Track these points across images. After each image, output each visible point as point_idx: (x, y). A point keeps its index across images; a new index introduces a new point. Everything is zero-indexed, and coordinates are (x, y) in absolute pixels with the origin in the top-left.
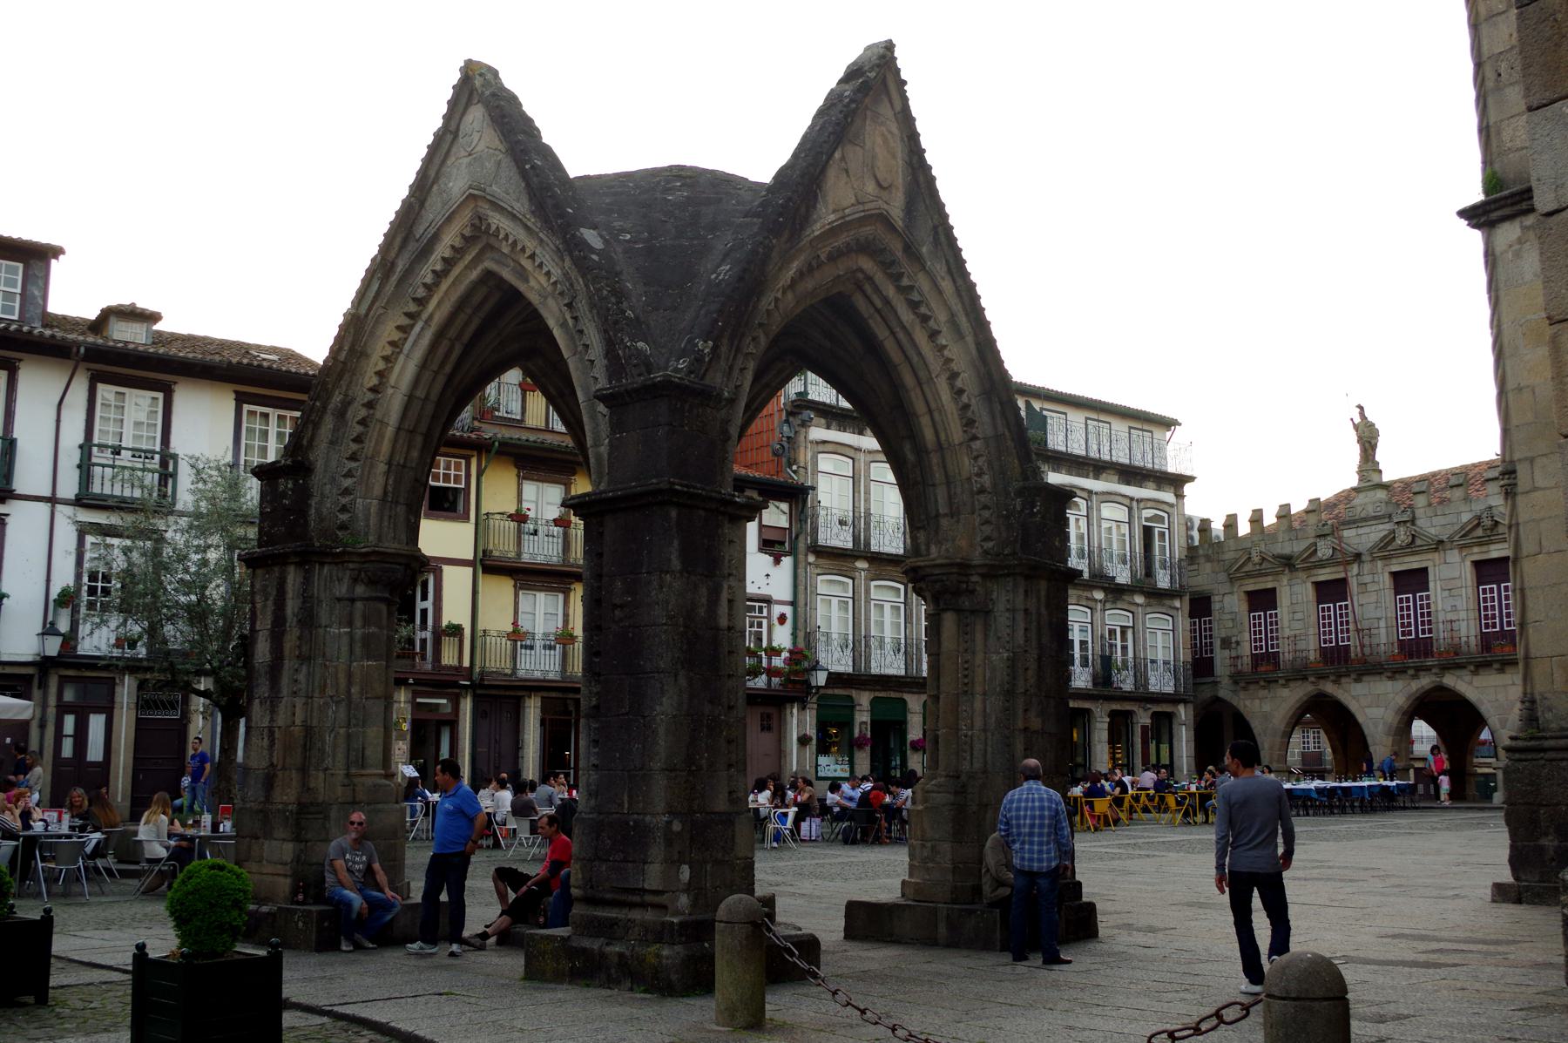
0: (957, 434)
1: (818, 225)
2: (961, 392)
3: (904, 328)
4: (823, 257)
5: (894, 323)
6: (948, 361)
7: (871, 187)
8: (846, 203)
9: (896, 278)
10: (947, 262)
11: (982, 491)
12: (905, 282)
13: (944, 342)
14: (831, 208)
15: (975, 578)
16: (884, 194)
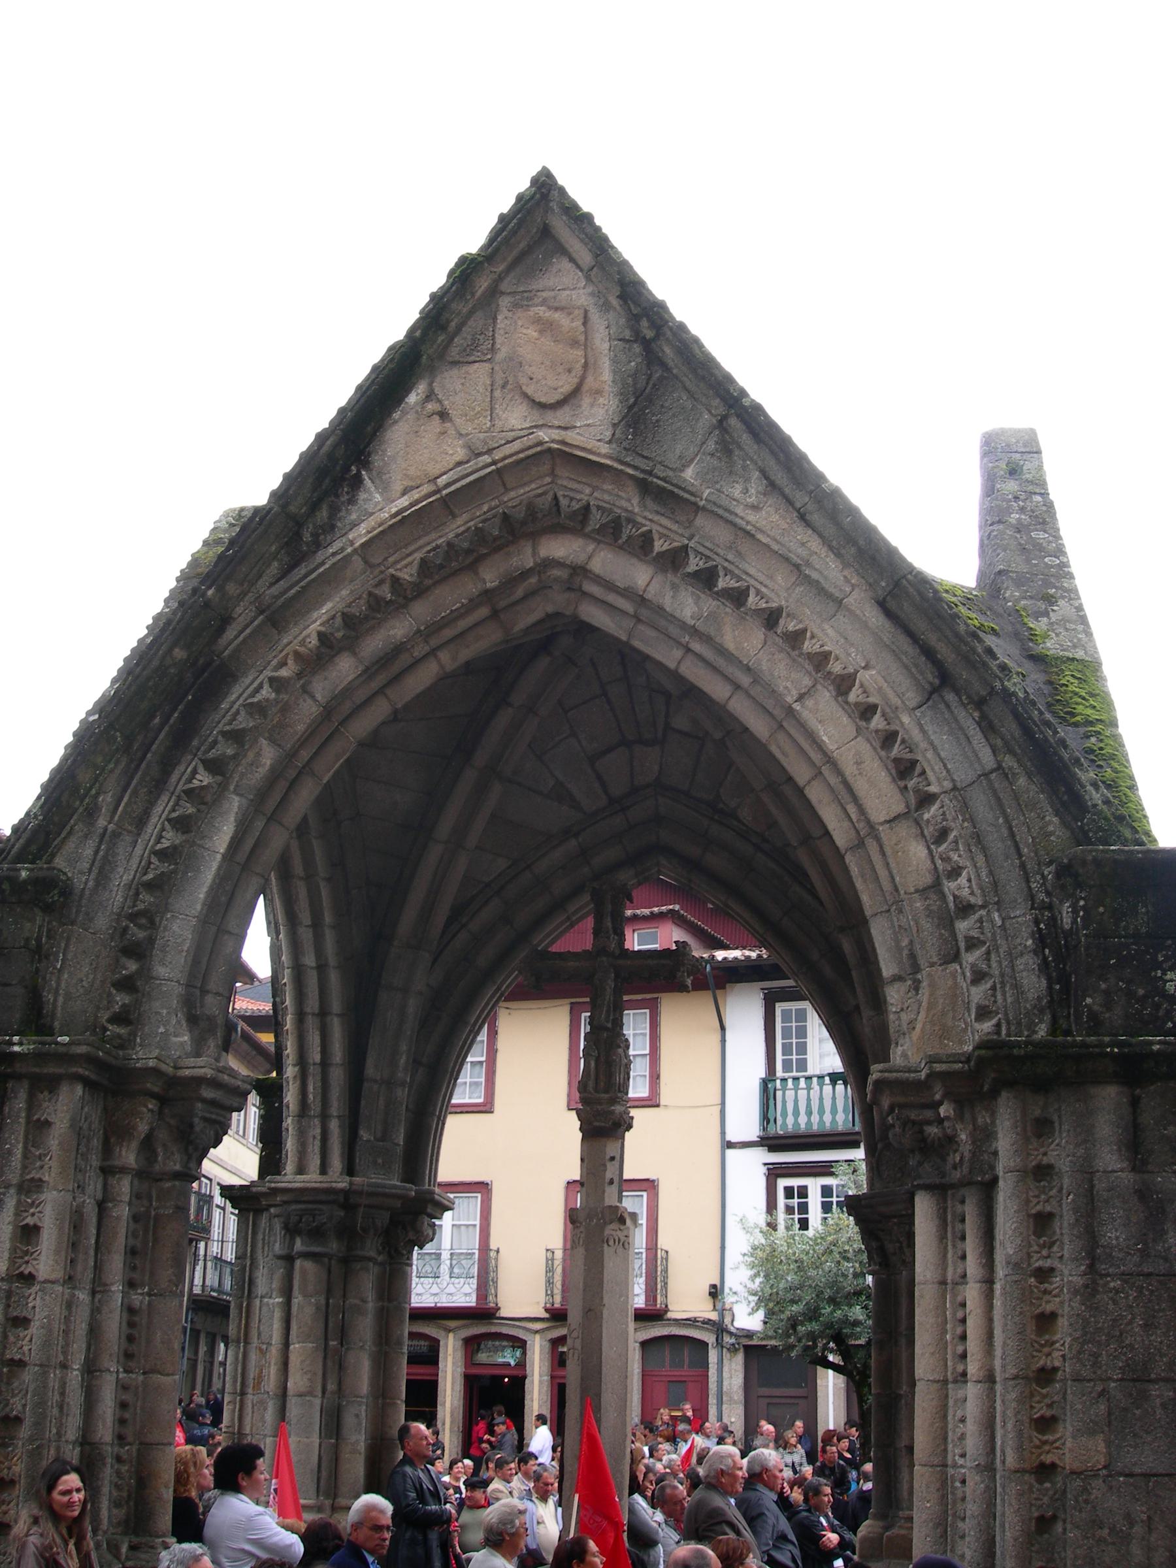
0: (881, 796)
1: (363, 528)
2: (867, 712)
3: (695, 632)
4: (408, 574)
5: (673, 630)
6: (821, 660)
7: (516, 417)
8: (434, 470)
9: (642, 546)
10: (764, 474)
11: (965, 909)
12: (659, 546)
13: (792, 626)
14: (398, 487)
15: (942, 1111)
16: (561, 416)
